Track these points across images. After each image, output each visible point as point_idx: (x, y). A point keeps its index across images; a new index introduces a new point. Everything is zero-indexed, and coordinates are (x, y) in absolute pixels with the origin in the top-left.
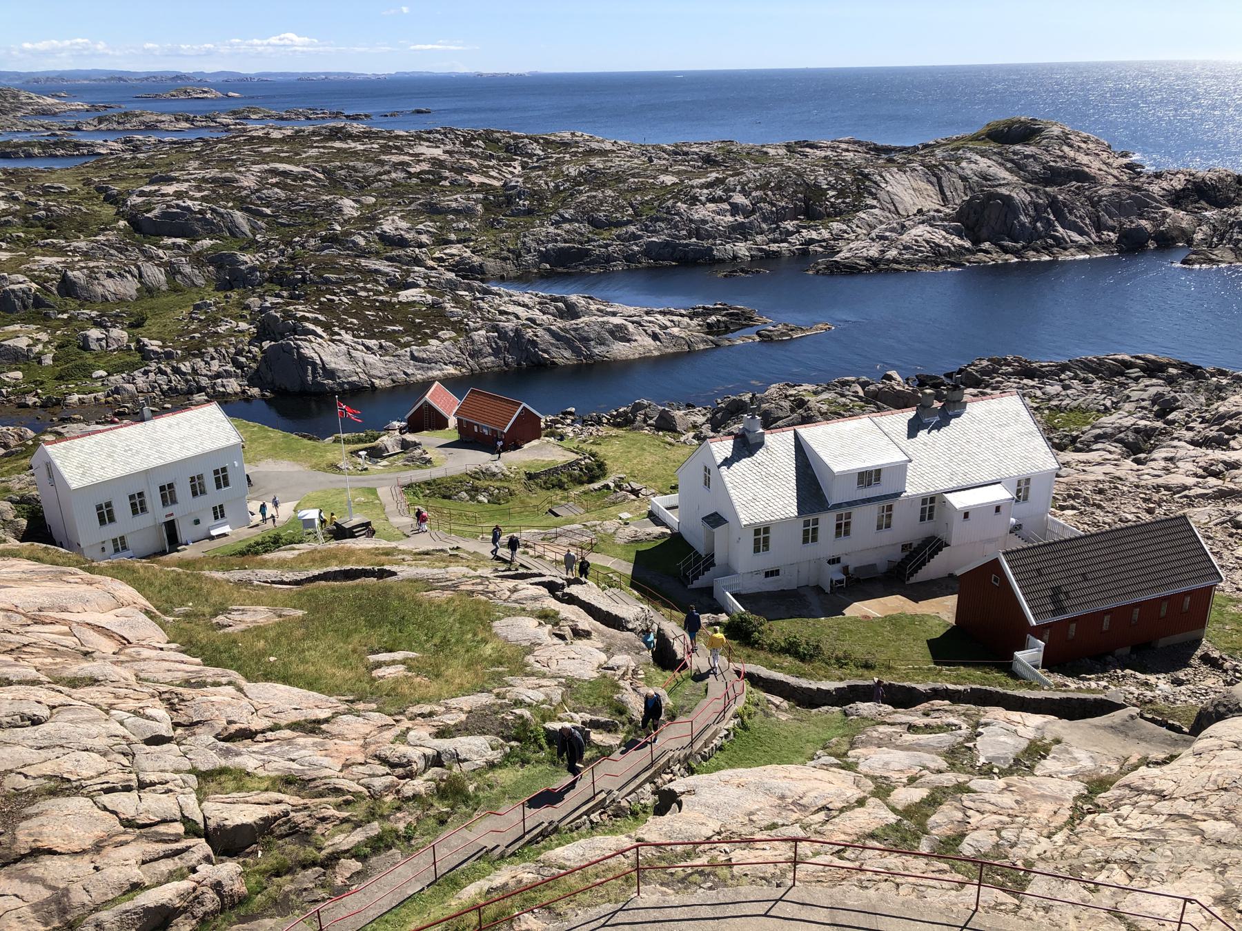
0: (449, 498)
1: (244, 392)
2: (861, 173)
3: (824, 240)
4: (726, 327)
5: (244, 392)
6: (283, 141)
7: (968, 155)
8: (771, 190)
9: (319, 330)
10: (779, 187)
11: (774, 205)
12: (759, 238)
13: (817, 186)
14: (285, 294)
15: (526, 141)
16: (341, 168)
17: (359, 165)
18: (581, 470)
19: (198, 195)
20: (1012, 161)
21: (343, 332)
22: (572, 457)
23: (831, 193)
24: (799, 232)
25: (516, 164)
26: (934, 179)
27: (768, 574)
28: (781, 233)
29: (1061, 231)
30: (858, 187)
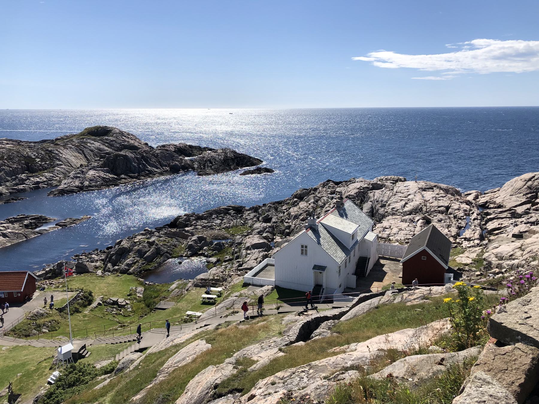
0: (29, 336)
2: (47, 150)
3: (44, 182)
4: (36, 225)
7: (89, 141)
8: (6, 159)
10: (10, 158)
11: (11, 167)
12: (8, 184)
13: (30, 157)
18: (82, 299)
20: (107, 143)
22: (74, 294)
23: (38, 160)
24: (29, 179)
26: (81, 152)
27: (340, 286)
28: (19, 180)
29: (150, 168)
30: (49, 156)
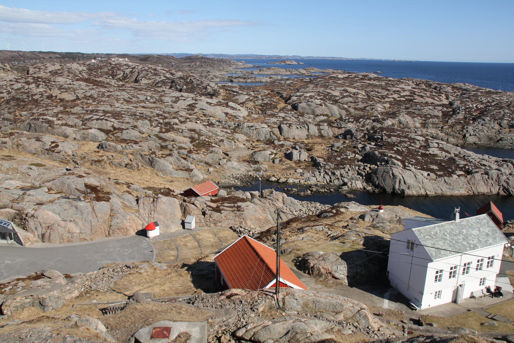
1: (364, 188)
5: (364, 188)
6: (343, 79)
9: (399, 163)
14: (373, 144)
15: (445, 86)
16: (372, 91)
17: (380, 91)
19: (319, 98)
21: (410, 165)
25: (443, 95)
